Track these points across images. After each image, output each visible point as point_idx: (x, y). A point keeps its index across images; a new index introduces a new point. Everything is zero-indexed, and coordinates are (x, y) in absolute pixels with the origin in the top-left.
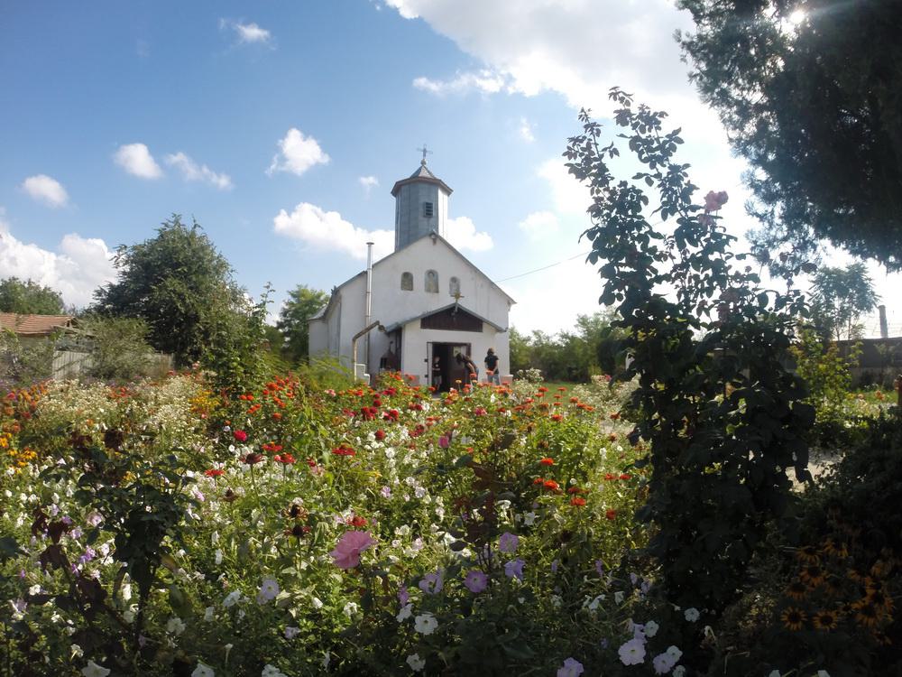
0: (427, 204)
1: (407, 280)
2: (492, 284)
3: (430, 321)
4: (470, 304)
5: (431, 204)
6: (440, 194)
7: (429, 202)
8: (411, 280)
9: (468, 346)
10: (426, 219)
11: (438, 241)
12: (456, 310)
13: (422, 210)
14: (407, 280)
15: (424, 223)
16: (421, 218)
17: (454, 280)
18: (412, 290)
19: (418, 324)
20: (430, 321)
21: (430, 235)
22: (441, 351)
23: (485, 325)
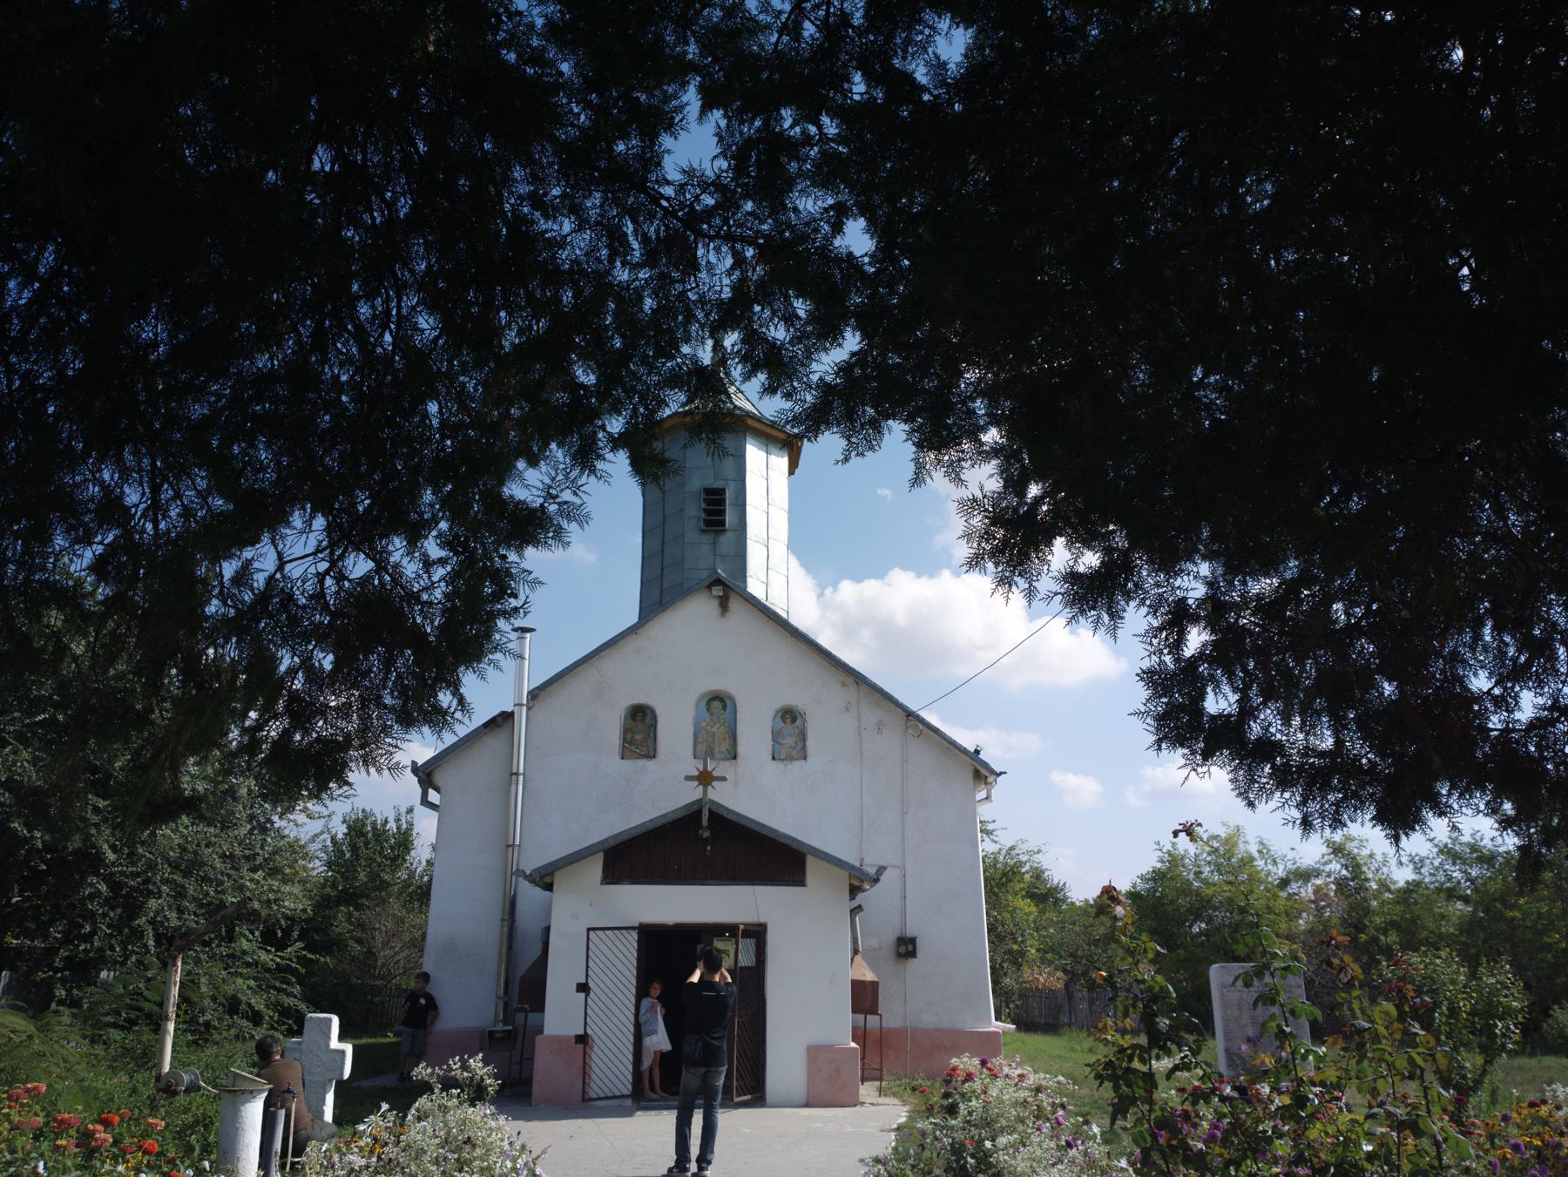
0: (709, 492)
1: (640, 728)
2: (910, 715)
3: (632, 858)
4: (760, 793)
5: (721, 492)
6: (754, 455)
7: (718, 484)
9: (757, 933)
11: (735, 604)
12: (705, 821)
13: (694, 511)
14: (640, 728)
15: (701, 553)
17: (789, 715)
18: (651, 755)
19: (596, 867)
20: (632, 858)
21: (709, 587)
22: (665, 954)
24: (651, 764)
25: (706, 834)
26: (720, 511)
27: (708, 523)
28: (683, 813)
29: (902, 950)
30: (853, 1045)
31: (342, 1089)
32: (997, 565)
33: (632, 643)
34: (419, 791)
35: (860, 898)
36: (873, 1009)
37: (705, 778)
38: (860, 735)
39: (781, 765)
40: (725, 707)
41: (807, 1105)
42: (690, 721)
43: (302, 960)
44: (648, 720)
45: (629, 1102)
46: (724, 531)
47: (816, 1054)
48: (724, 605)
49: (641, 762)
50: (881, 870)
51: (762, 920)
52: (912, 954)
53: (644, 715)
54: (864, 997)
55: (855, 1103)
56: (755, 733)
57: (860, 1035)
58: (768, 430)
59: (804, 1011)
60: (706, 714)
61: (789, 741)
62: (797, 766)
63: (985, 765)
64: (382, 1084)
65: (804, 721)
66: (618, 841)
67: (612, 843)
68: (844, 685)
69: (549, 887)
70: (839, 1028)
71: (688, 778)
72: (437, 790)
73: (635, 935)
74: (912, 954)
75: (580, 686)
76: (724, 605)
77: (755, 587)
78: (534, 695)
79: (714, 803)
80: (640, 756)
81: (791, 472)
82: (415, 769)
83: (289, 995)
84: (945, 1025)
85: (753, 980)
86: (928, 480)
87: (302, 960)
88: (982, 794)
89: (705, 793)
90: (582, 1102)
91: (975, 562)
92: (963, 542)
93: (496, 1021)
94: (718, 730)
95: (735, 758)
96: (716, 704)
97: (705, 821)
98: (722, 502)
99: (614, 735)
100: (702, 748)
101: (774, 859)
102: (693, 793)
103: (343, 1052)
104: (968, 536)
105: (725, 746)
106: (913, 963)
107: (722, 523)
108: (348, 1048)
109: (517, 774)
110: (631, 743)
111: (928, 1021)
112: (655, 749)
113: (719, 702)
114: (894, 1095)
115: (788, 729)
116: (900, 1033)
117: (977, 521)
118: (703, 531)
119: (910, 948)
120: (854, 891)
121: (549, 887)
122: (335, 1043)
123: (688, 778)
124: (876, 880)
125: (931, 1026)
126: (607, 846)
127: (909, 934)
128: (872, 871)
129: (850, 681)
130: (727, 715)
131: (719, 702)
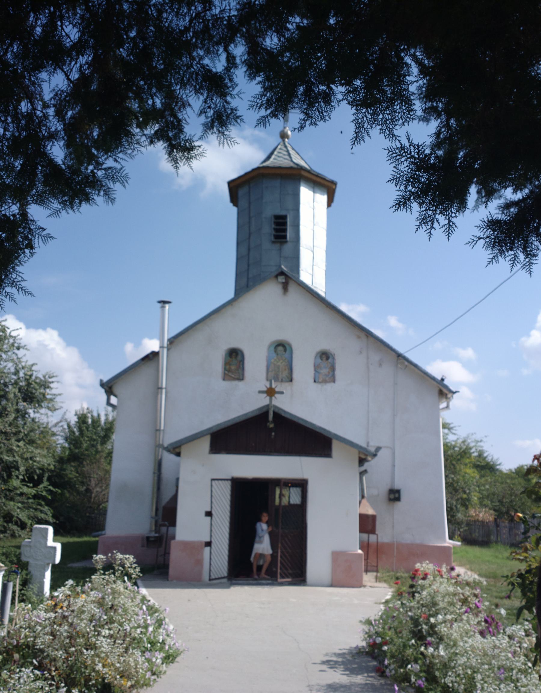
2: (399, 356)
3: (228, 438)
4: (305, 402)
5: (284, 217)
6: (306, 193)
7: (283, 213)
8: (242, 361)
9: (302, 485)
10: (278, 245)
11: (292, 287)
13: (268, 229)
16: (266, 244)
17: (325, 355)
18: (241, 378)
19: (206, 443)
20: (228, 438)
21: (276, 277)
23: (336, 446)
24: (240, 384)
25: (272, 426)
26: (283, 230)
27: (276, 237)
29: (392, 496)
30: (360, 551)
31: (54, 566)
32: (420, 205)
33: (229, 311)
34: (105, 397)
35: (366, 466)
36: (373, 531)
37: (271, 392)
38: (368, 367)
39: (319, 386)
40: (285, 350)
41: (332, 586)
43: (50, 492)
44: (239, 358)
45: (225, 580)
46: (286, 242)
47: (337, 557)
48: (285, 287)
50: (378, 449)
51: (305, 477)
52: (398, 499)
54: (367, 524)
55: (360, 585)
56: (303, 365)
57: (365, 546)
58: (314, 178)
59: (330, 531)
60: (274, 355)
61: (324, 371)
62: (329, 387)
63: (446, 387)
64: (75, 568)
65: (334, 359)
66: (218, 428)
67: (215, 430)
68: (359, 337)
69: (178, 454)
70: (351, 541)
71: (260, 392)
72: (115, 396)
73: (228, 484)
74: (398, 499)
75: (200, 336)
76: (285, 287)
77: (305, 277)
78: (172, 341)
79: (275, 407)
81: (329, 204)
82: (102, 385)
83: (42, 512)
84: (418, 541)
85: (300, 511)
86: (367, 138)
87: (50, 492)
88: (443, 405)
89: (271, 401)
90: (193, 580)
91: (402, 203)
92: (392, 185)
93: (151, 531)
94: (281, 364)
95: (291, 380)
96: (280, 348)
98: (285, 224)
100: (271, 374)
101: (314, 442)
102: (263, 401)
103: (55, 548)
104: (396, 180)
105: (285, 374)
106: (398, 504)
107: (285, 237)
108: (59, 546)
109: (161, 388)
110: (229, 371)
111: (408, 538)
112: (243, 375)
114: (385, 581)
116: (390, 546)
117: (404, 167)
118: (273, 242)
119: (397, 495)
120: (362, 461)
121: (178, 454)
122: (50, 542)
123: (260, 392)
124: (375, 455)
125: (409, 542)
126: (211, 431)
127: (396, 487)
128: (373, 450)
129: (362, 335)
130: (287, 355)
131: (282, 347)
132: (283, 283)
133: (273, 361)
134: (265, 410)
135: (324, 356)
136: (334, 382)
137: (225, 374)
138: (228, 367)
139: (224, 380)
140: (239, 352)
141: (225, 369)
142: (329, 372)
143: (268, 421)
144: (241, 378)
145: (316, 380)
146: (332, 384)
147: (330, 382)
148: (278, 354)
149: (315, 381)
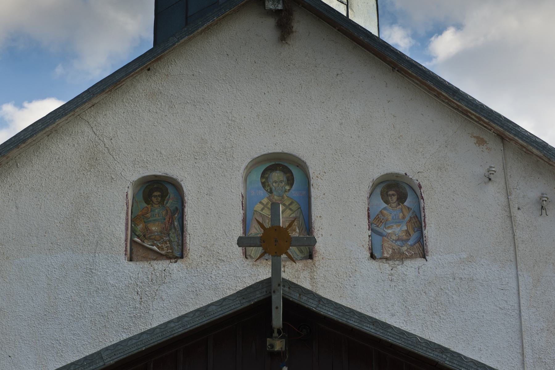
1: (158, 214)
12: (277, 320)
14: (158, 214)
18: (178, 253)
24: (175, 267)
25: (279, 345)
28: (237, 306)
39: (386, 266)
40: (290, 181)
42: (238, 201)
44: (170, 203)
49: (161, 265)
53: (164, 195)
56: (340, 222)
60: (262, 192)
61: (397, 230)
62: (410, 268)
65: (419, 198)
68: (481, 142)
76: (284, 30)
80: (160, 256)
89: (276, 269)
96: (277, 176)
97: (277, 320)
99: (118, 229)
110: (144, 237)
113: (281, 170)
115: (393, 212)
130: (295, 192)
132: (278, 12)
133: (258, 207)
134: (259, 296)
135: (391, 193)
136: (424, 257)
137: (132, 241)
138: (140, 226)
139: (131, 260)
140: (170, 190)
141: (133, 231)
142: (407, 232)
143: (269, 330)
144: (177, 254)
145: (376, 255)
146: (420, 262)
147: (411, 257)
148: (271, 192)
149: (372, 256)
